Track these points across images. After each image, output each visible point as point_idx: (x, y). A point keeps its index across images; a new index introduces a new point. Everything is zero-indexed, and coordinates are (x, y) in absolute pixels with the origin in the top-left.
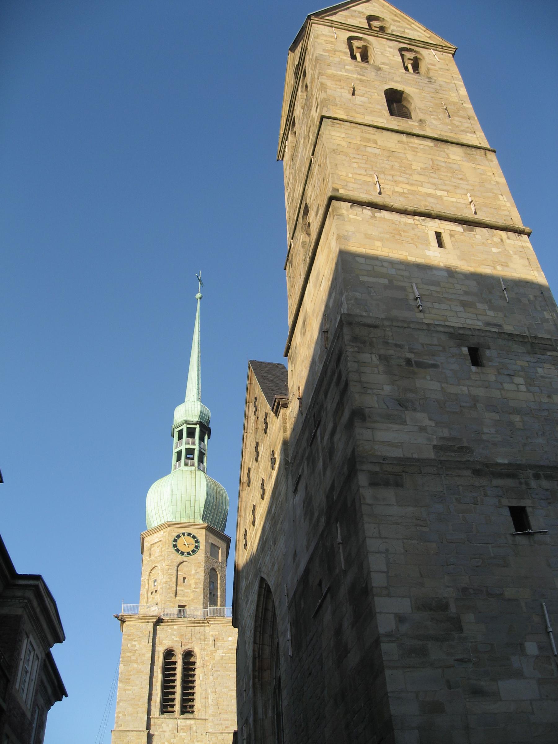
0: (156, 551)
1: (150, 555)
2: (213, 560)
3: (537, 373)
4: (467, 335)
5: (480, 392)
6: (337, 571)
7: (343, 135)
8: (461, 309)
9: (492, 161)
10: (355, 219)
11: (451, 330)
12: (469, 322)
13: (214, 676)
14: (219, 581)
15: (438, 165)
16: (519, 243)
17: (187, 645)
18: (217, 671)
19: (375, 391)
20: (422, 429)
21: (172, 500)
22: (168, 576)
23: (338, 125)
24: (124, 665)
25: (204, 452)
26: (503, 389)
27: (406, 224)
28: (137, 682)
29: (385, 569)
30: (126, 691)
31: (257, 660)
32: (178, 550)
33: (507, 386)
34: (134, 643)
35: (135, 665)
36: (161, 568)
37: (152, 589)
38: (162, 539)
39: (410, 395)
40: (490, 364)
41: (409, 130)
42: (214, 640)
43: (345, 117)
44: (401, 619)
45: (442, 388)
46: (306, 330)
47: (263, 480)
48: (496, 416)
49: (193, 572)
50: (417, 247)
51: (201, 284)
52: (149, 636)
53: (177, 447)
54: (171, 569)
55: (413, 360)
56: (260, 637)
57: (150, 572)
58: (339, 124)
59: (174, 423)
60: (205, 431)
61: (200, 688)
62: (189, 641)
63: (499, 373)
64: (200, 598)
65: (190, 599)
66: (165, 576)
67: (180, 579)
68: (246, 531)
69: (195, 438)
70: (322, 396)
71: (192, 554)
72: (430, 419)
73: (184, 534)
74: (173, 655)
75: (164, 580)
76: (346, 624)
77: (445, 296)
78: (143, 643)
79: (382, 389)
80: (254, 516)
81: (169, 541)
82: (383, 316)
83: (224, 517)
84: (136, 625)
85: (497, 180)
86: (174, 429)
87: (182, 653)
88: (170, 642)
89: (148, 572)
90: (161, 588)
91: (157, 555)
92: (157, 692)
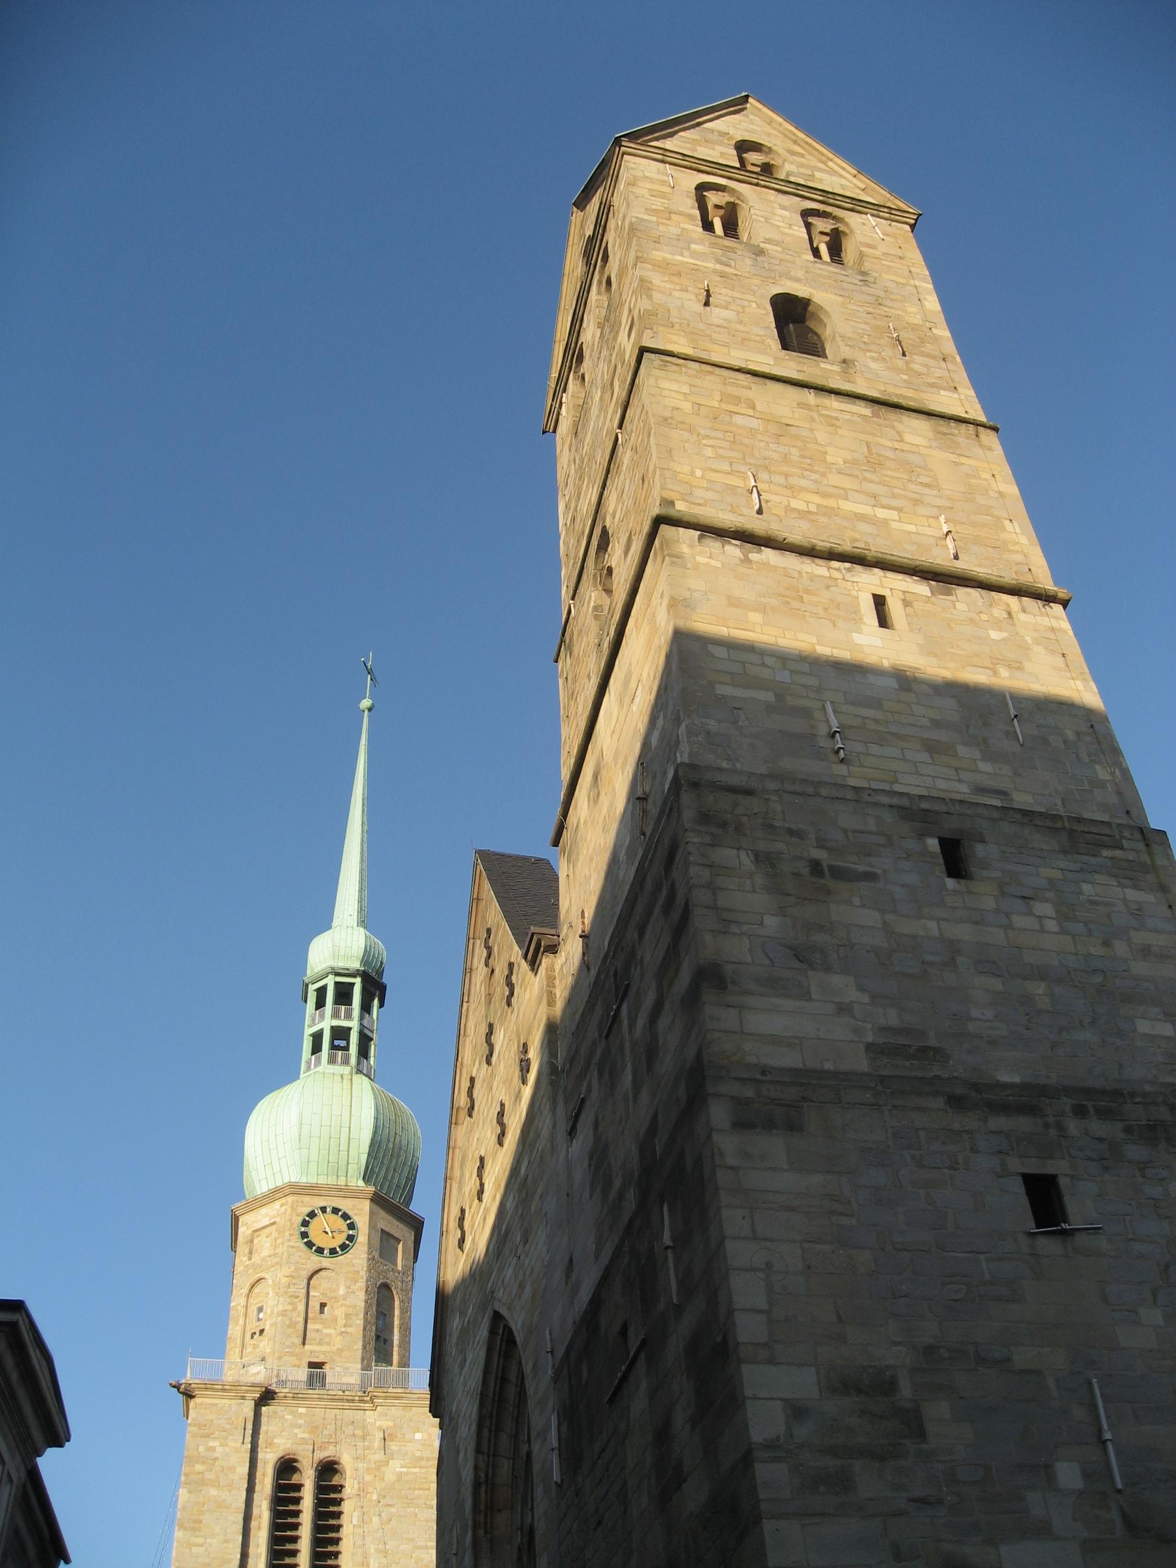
0: (264, 1245)
1: (251, 1253)
2: (386, 1265)
3: (1081, 893)
4: (938, 812)
5: (963, 932)
6: (662, 1305)
7: (686, 389)
8: (924, 757)
9: (990, 449)
10: (708, 564)
11: (905, 802)
12: (941, 784)
13: (383, 1515)
14: (397, 1312)
15: (880, 455)
16: (1045, 621)
17: (325, 1449)
18: (389, 1505)
19: (745, 928)
20: (844, 1009)
21: (300, 1136)
23: (675, 368)
24: (189, 1492)
25: (370, 1034)
26: (1009, 927)
27: (812, 577)
28: (217, 1529)
29: (766, 1307)
30: (193, 1548)
31: (483, 1488)
32: (310, 1245)
33: (1019, 921)
34: (212, 1444)
35: (213, 1492)
36: (273, 1281)
37: (253, 1326)
38: (278, 1219)
39: (818, 938)
40: (985, 873)
41: (820, 382)
42: (385, 1439)
43: (689, 351)
44: (796, 1411)
45: (885, 923)
46: (599, 794)
47: (502, 1105)
48: (997, 984)
49: (342, 1291)
50: (834, 625)
51: (371, 679)
52: (245, 1429)
53: (313, 1023)
54: (294, 1284)
55: (825, 864)
56: (489, 1440)
57: (250, 1290)
58: (677, 365)
59: (309, 973)
60: (372, 989)
61: (352, 1541)
62: (331, 1440)
63: (1003, 893)
64: (355, 1347)
65: (334, 1349)
66: (282, 1300)
67: (315, 1305)
68: (463, 1211)
69: (351, 1005)
70: (632, 934)
71: (340, 1252)
72: (861, 989)
73: (323, 1209)
74: (295, 1470)
75: (280, 1308)
76: (680, 1418)
77: (893, 729)
78: (232, 1444)
79: (761, 924)
80: (481, 1179)
81: (292, 1224)
82: (763, 770)
83: (411, 1174)
84: (217, 1404)
85: (1001, 490)
86: (307, 985)
87: (315, 1465)
88: (290, 1441)
89: (245, 1291)
91: (265, 1253)
92: (259, 1551)
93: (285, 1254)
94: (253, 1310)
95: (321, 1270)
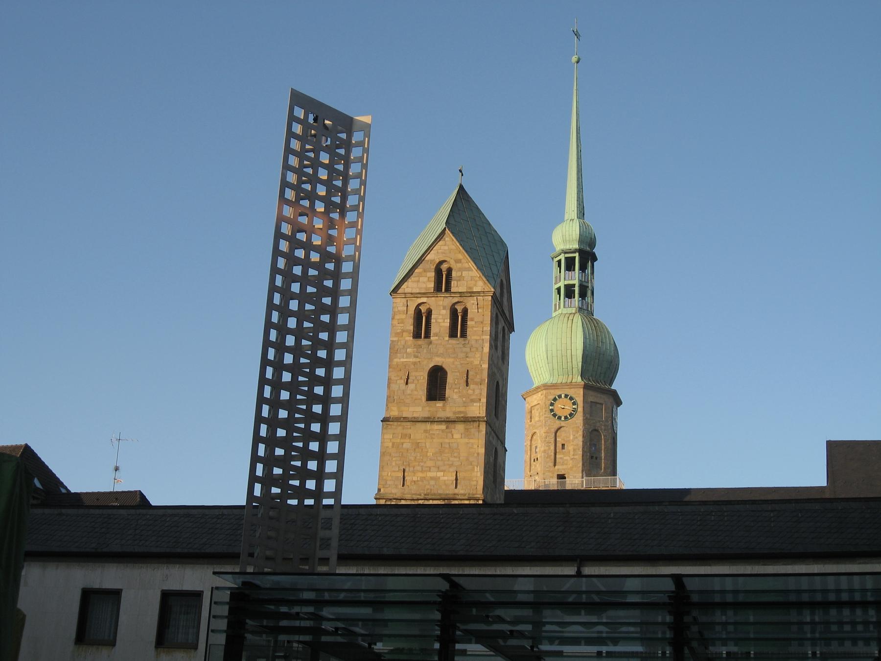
1: (531, 418)
22: (546, 444)
32: (555, 415)
36: (540, 435)
38: (540, 402)
49: (571, 438)
54: (549, 436)
57: (532, 437)
64: (579, 466)
65: (569, 466)
66: (543, 445)
73: (560, 396)
75: (542, 449)
81: (545, 405)
90: (541, 457)
91: (537, 419)
93: (544, 421)
94: (533, 447)
95: (561, 427)
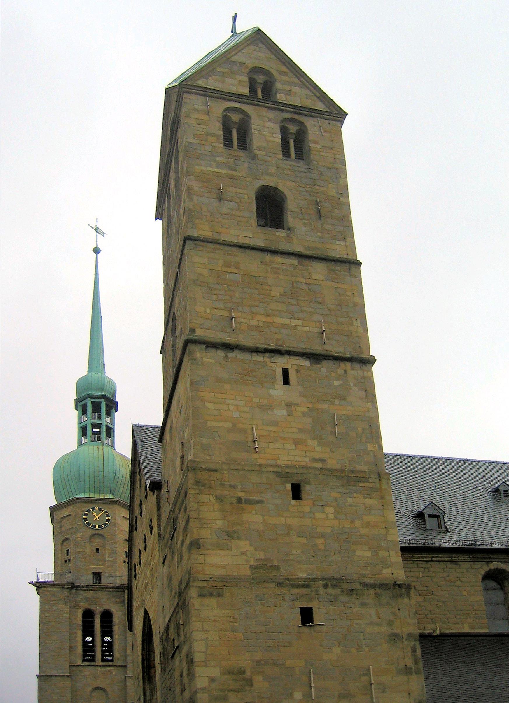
5: (294, 521)
11: (279, 470)
19: (209, 525)
33: (318, 515)
45: (264, 520)
47: (145, 536)
48: (304, 541)
63: (314, 505)
79: (216, 523)
